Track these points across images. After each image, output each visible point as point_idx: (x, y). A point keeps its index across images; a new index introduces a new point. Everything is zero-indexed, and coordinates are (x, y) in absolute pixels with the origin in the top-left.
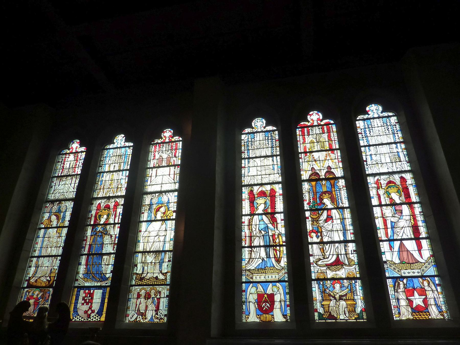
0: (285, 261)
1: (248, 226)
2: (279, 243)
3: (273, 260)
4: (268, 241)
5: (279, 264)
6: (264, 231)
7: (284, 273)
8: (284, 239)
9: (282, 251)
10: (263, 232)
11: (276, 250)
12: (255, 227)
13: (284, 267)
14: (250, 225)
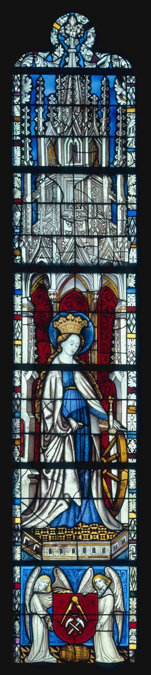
0: (131, 511)
1: (30, 403)
2: (118, 456)
3: (99, 505)
4: (87, 451)
5: (114, 518)
6: (77, 421)
7: (126, 540)
8: (133, 446)
9: (126, 481)
10: (74, 424)
11: (108, 479)
12: (50, 406)
13: (129, 526)
14: (36, 397)
